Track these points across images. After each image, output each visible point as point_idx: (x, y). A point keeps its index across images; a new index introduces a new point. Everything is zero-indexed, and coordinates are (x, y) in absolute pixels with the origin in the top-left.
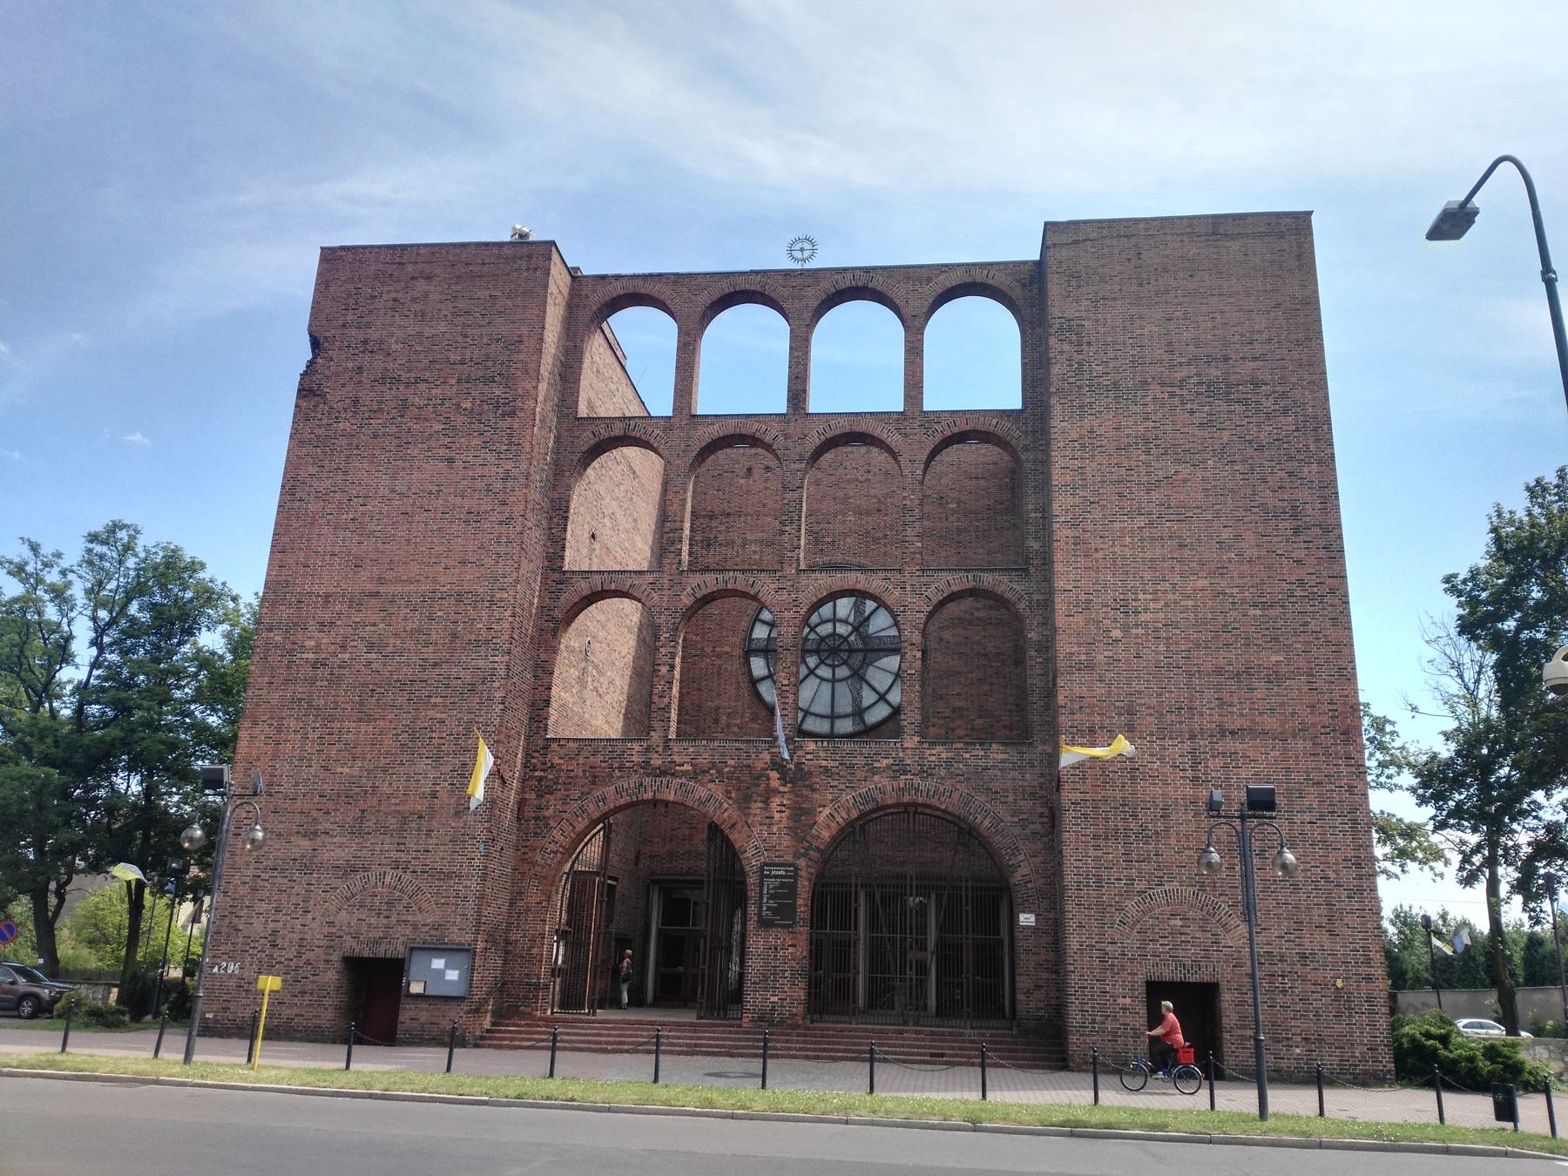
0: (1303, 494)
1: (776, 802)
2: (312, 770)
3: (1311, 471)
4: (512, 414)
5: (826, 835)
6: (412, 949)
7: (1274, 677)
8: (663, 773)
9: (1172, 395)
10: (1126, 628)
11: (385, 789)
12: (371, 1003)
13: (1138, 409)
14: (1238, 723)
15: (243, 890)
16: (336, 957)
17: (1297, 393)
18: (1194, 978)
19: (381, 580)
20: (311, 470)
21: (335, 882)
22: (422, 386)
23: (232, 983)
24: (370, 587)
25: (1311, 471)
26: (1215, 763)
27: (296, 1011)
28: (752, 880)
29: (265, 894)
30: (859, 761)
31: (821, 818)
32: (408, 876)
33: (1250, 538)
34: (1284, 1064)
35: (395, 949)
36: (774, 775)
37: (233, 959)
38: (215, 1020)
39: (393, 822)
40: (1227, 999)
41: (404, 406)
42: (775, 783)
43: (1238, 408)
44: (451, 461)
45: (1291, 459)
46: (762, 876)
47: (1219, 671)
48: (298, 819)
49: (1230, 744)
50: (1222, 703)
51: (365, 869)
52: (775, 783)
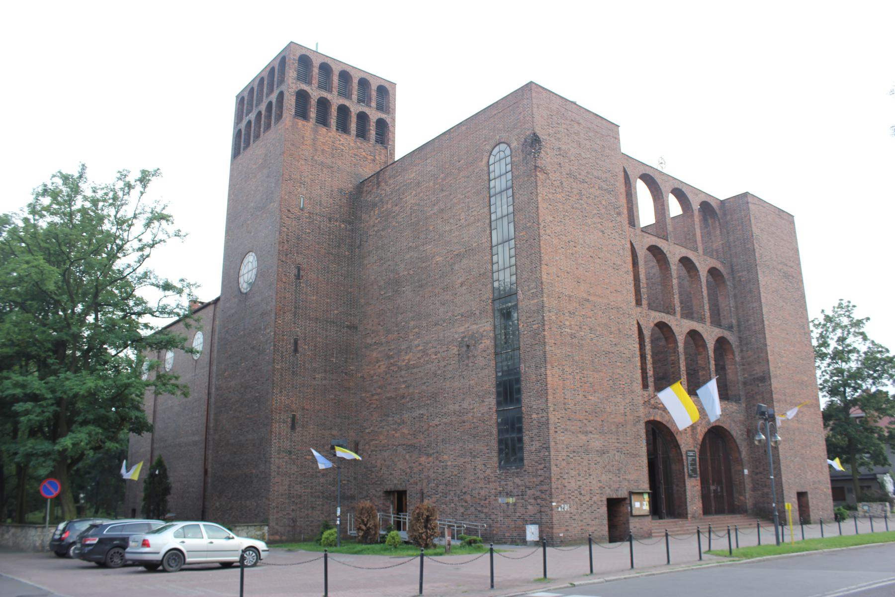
2: (580, 397)
6: (631, 493)
8: (655, 408)
11: (608, 410)
15: (564, 464)
16: (604, 499)
20: (551, 219)
21: (599, 459)
22: (586, 185)
23: (568, 516)
24: (585, 296)
27: (594, 528)
28: (684, 457)
29: (572, 466)
32: (623, 456)
35: (622, 494)
37: (565, 502)
38: (564, 537)
39: (613, 428)
41: (580, 193)
46: (687, 456)
48: (579, 424)
51: (608, 452)
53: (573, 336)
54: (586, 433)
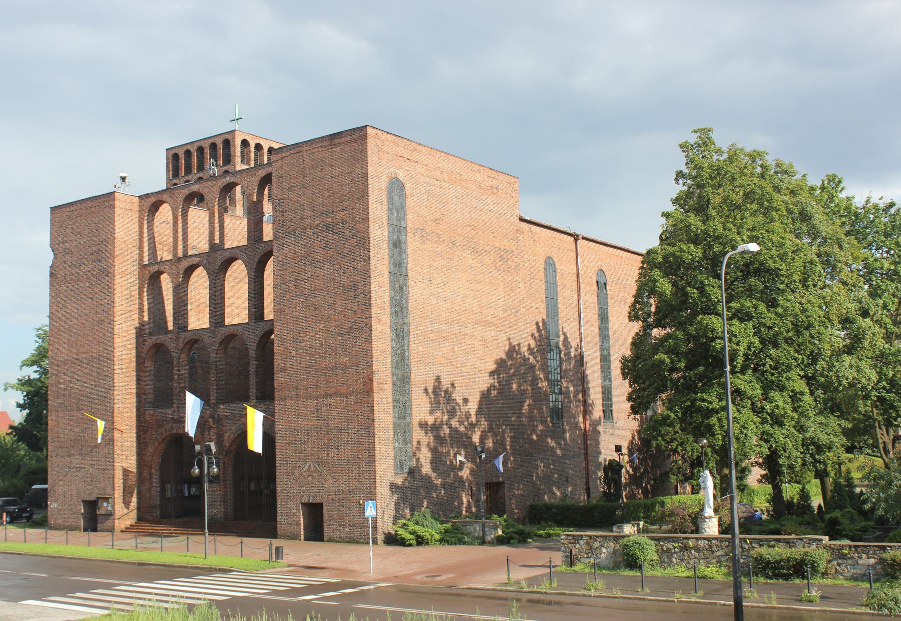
0: (358, 278)
1: (212, 431)
3: (360, 266)
4: (107, 275)
5: (228, 445)
7: (345, 368)
9: (314, 233)
10: (296, 350)
12: (94, 518)
13: (301, 242)
14: (333, 390)
17: (357, 226)
18: (315, 501)
19: (78, 353)
24: (75, 356)
25: (360, 266)
26: (324, 409)
30: (237, 412)
31: (226, 438)
33: (339, 302)
34: (342, 535)
36: (211, 420)
40: (325, 508)
42: (211, 424)
43: (336, 237)
44: (92, 298)
45: (354, 260)
47: (326, 367)
49: (331, 401)
50: (327, 382)
52: (211, 424)
53: (65, 389)
54: (70, 456)
